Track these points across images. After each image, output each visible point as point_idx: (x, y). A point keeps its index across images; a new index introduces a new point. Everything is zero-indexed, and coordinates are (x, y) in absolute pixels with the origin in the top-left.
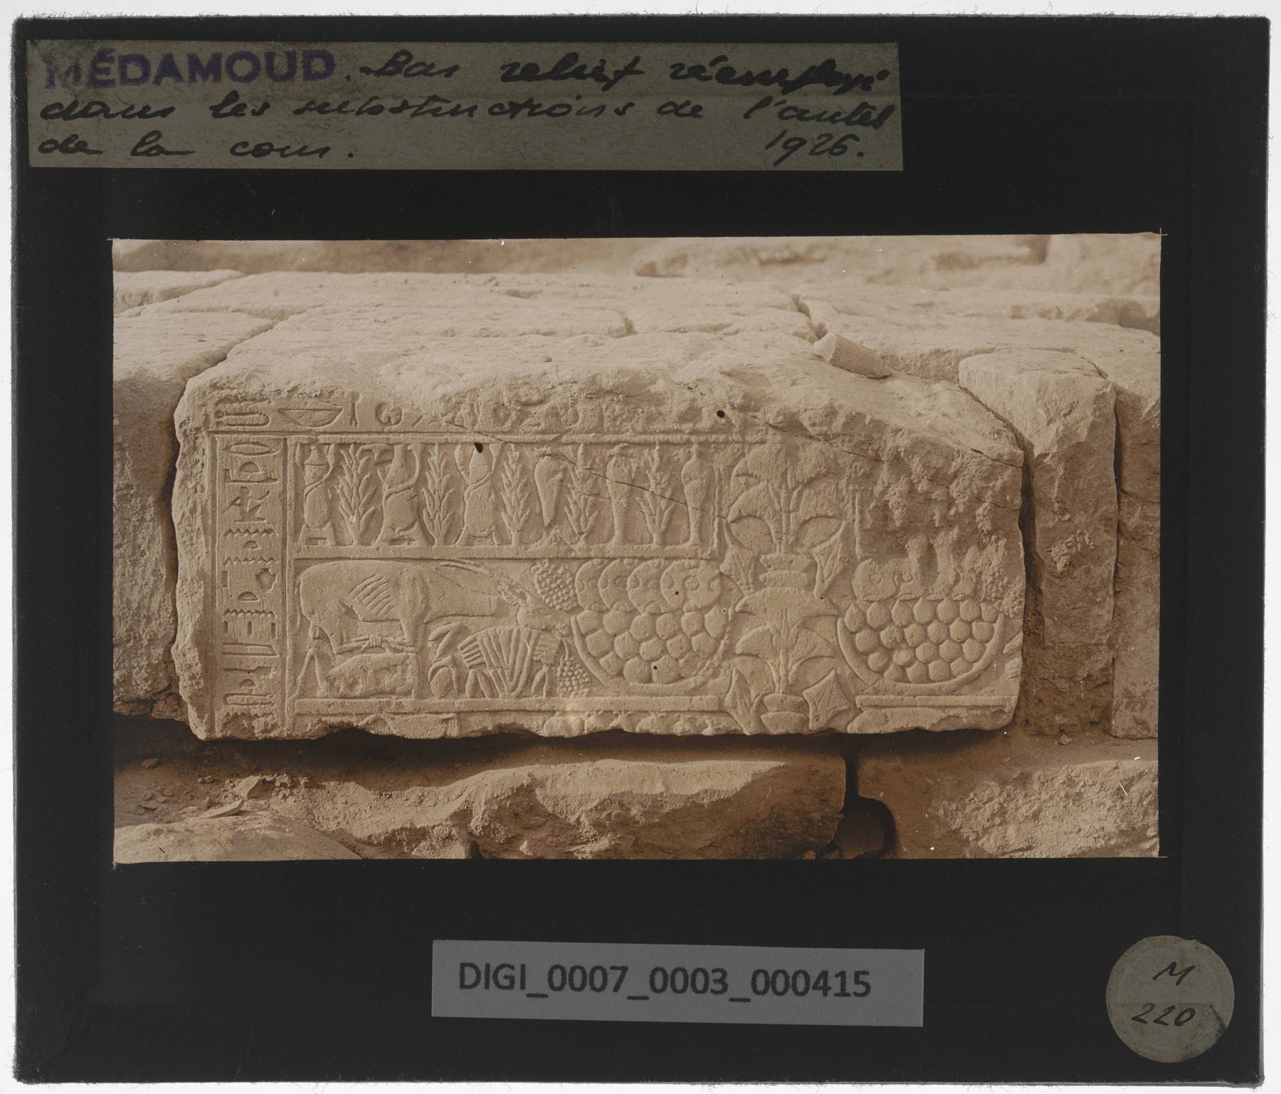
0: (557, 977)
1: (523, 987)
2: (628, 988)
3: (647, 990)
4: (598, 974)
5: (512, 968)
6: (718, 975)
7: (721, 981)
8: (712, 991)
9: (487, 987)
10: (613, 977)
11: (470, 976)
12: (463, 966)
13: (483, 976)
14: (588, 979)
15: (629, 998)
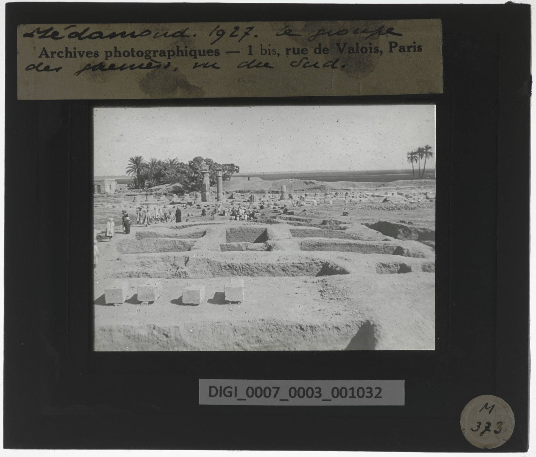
0: (250, 391)
1: (236, 396)
2: (280, 396)
3: (287, 397)
4: (267, 390)
5: (231, 388)
6: (318, 390)
7: (319, 392)
8: (316, 397)
9: (221, 396)
10: (274, 391)
11: (214, 392)
12: (211, 387)
13: (219, 392)
14: (263, 392)
15: (280, 400)
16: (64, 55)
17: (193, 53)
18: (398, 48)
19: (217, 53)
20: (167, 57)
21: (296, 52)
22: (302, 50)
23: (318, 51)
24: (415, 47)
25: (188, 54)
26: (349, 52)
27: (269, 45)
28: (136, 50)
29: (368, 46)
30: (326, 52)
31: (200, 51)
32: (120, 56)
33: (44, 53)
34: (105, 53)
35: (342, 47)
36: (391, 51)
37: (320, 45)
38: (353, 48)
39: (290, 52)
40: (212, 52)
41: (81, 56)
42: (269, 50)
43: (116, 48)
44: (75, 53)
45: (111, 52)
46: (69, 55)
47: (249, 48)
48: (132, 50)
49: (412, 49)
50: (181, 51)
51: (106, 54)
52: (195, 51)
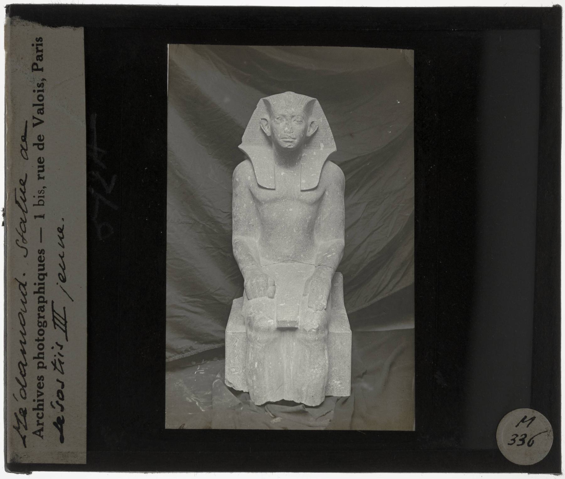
16: (40, 412)
17: (41, 277)
19: (41, 252)
20: (45, 304)
21: (41, 169)
22: (40, 162)
23: (41, 147)
24: (37, 45)
26: (42, 114)
28: (37, 336)
29: (37, 94)
30: (42, 138)
31: (39, 270)
32: (43, 353)
33: (38, 433)
34: (40, 369)
35: (39, 121)
36: (42, 70)
37: (34, 144)
38: (39, 109)
39: (42, 175)
40: (40, 257)
41: (42, 394)
42: (39, 197)
43: (34, 358)
44: (38, 401)
45: (38, 364)
47: (37, 218)
48: (38, 340)
49: (40, 48)
50: (39, 290)
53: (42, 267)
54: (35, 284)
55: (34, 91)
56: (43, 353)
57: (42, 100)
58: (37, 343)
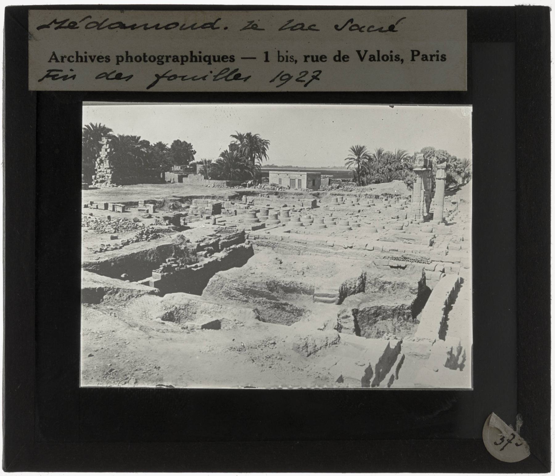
16: (75, 59)
17: (207, 59)
18: (420, 56)
19: (232, 59)
20: (180, 62)
21: (315, 59)
22: (321, 57)
23: (337, 58)
24: (438, 56)
25: (202, 60)
26: (370, 60)
27: (287, 52)
28: (148, 55)
30: (346, 59)
31: (214, 57)
32: (132, 61)
33: (53, 57)
36: (413, 60)
37: (339, 52)
38: (374, 56)
39: (309, 59)
40: (227, 58)
41: (92, 61)
42: (287, 56)
43: (127, 52)
44: (86, 57)
46: (79, 58)
47: (265, 55)
48: (145, 55)
49: (435, 58)
51: (118, 59)
52: (210, 57)
53: (217, 59)
54: (200, 52)
55: (391, 52)
56: (132, 61)
57: (383, 59)
58: (142, 56)
